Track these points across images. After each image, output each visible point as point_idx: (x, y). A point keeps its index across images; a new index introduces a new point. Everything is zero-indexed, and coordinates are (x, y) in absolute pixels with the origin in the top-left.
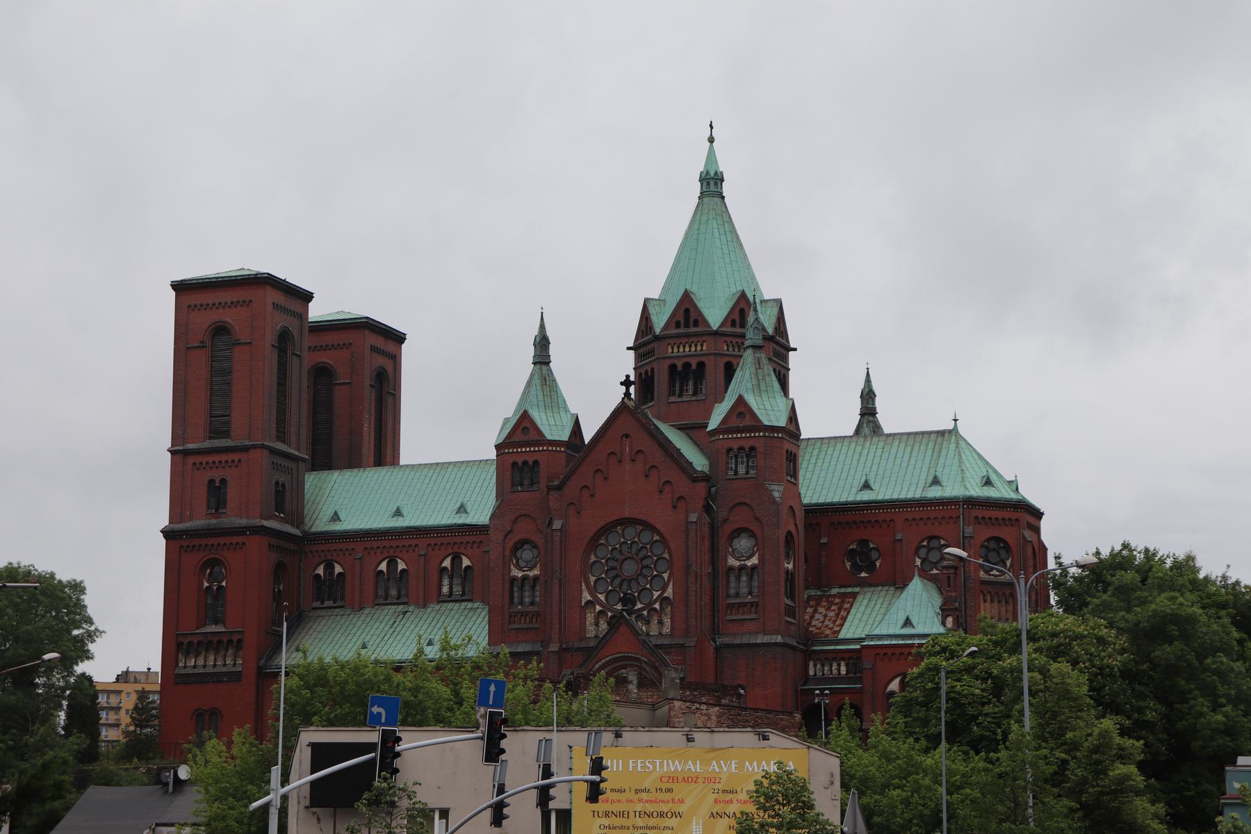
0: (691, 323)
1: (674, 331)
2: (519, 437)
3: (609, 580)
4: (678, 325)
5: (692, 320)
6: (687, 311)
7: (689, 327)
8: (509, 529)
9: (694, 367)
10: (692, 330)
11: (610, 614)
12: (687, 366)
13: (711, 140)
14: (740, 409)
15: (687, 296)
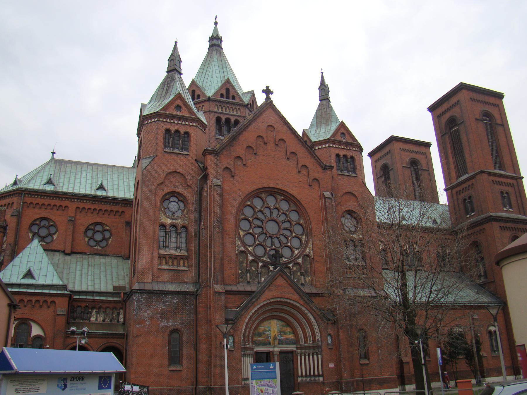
0: (231, 97)
1: (218, 98)
2: (172, 111)
3: (256, 236)
4: (222, 96)
5: (231, 95)
6: (228, 90)
7: (229, 99)
8: (162, 181)
9: (233, 121)
10: (230, 100)
11: (260, 264)
12: (228, 121)
13: (216, 23)
14: (342, 130)
15: (228, 81)
